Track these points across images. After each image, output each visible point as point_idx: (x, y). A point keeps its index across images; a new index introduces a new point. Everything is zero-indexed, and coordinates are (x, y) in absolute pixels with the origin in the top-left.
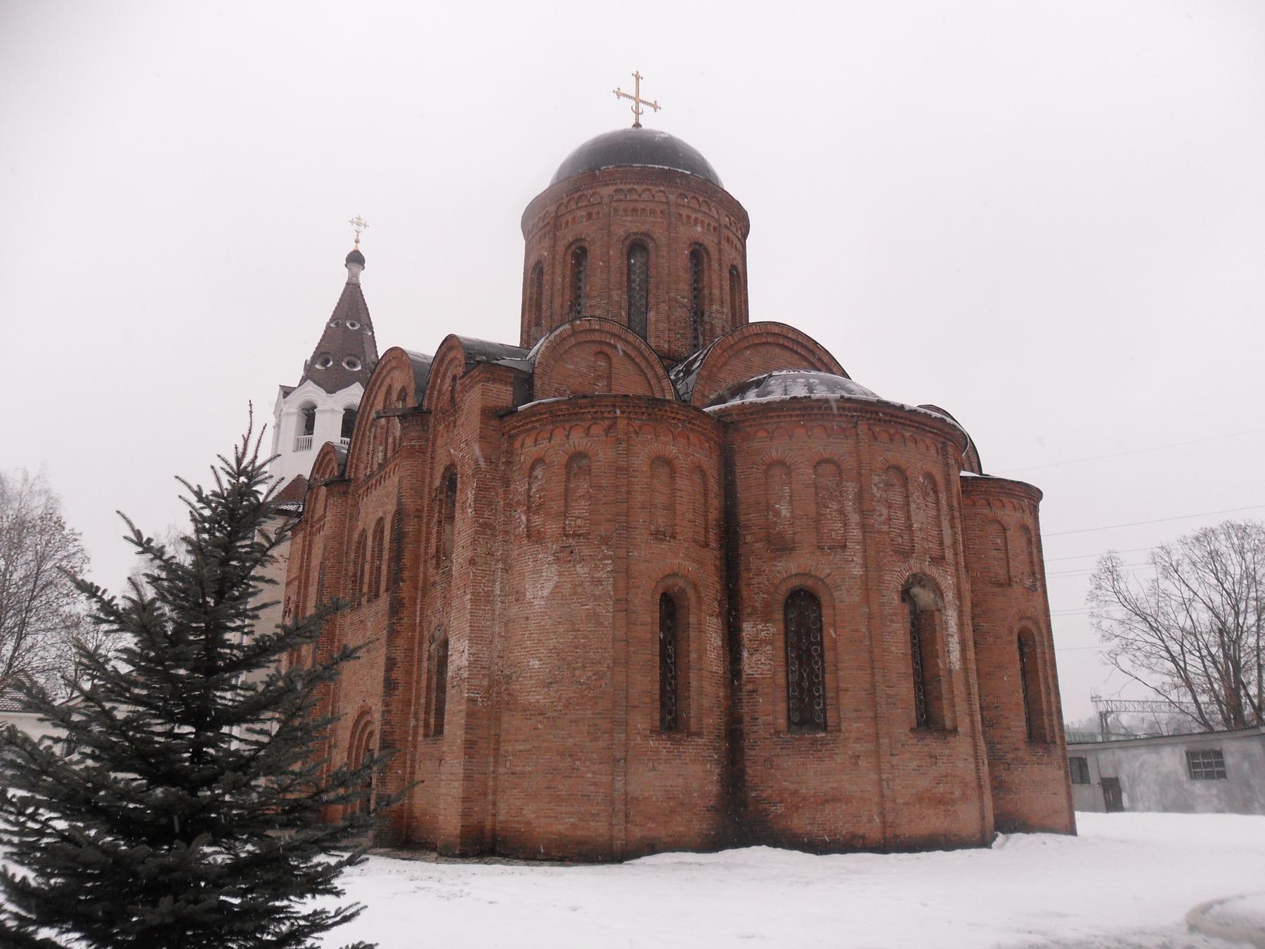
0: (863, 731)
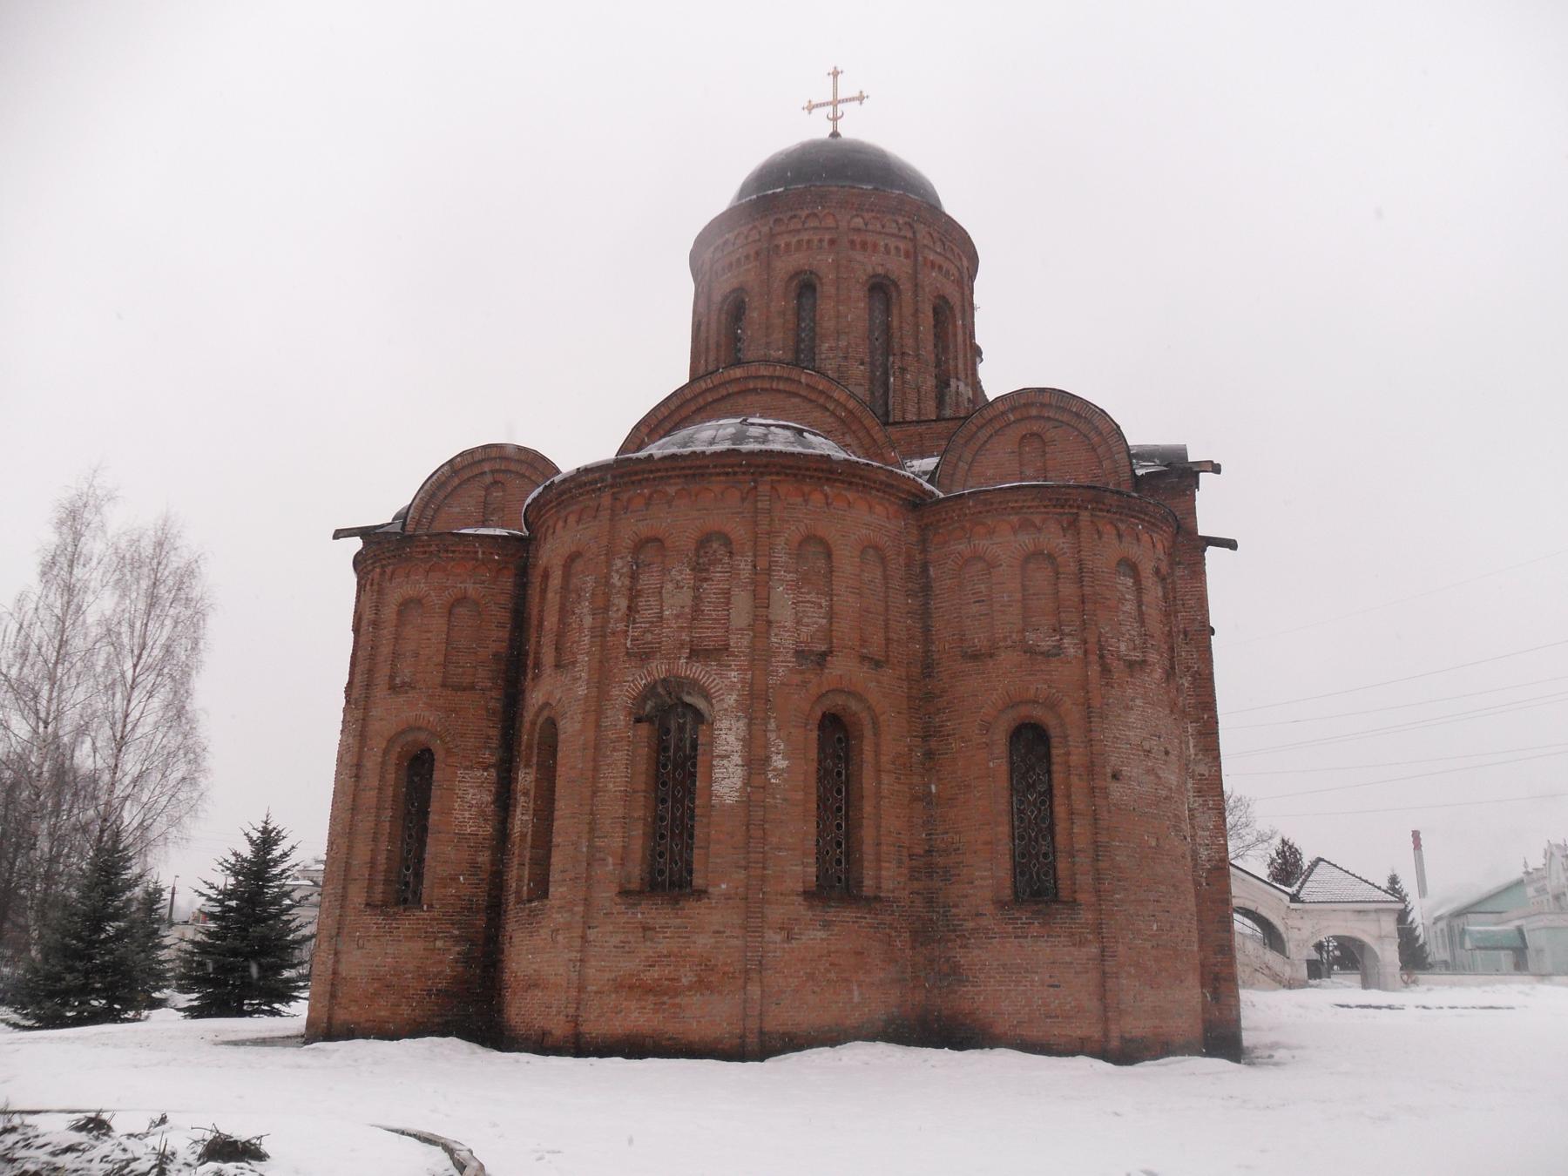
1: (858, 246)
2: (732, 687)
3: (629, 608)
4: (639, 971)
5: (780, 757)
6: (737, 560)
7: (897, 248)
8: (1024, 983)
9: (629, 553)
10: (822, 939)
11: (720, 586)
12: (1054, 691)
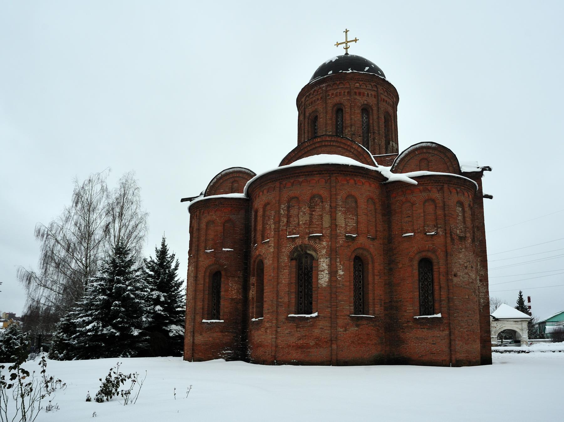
0: (269, 318)
1: (357, 94)
2: (324, 248)
3: (287, 221)
4: (295, 341)
5: (341, 271)
6: (324, 204)
7: (371, 94)
8: (424, 343)
9: (286, 202)
10: (356, 330)
11: (319, 213)
12: (435, 247)
